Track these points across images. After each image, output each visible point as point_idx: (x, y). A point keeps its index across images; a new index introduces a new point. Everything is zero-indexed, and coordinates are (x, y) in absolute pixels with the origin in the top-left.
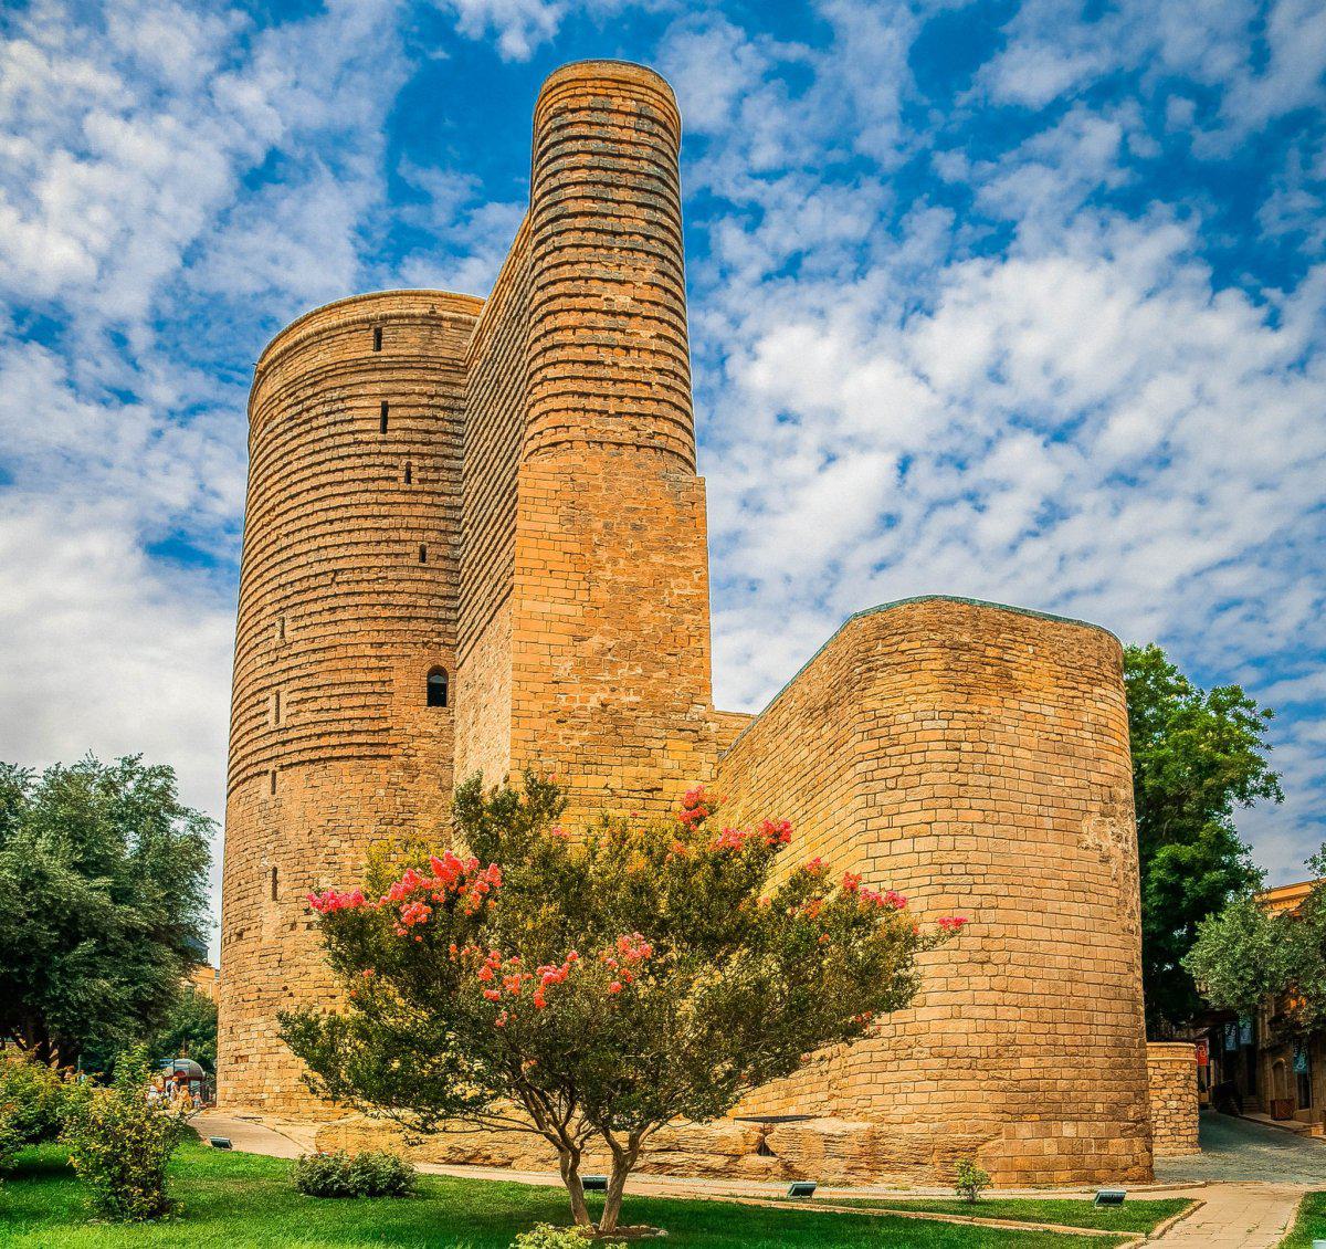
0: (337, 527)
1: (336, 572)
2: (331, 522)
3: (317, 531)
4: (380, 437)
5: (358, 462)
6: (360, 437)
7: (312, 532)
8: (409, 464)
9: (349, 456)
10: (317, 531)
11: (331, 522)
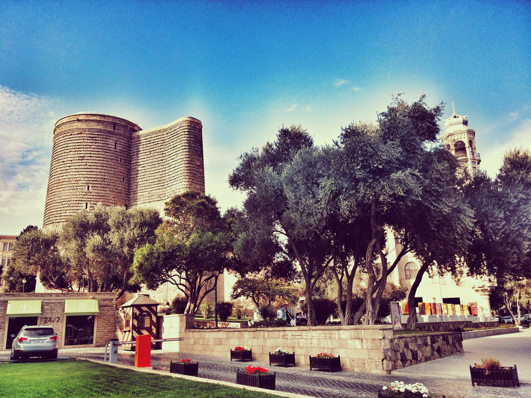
0: (104, 168)
1: (104, 179)
2: (103, 167)
3: (100, 168)
4: (115, 150)
5: (110, 154)
6: (111, 149)
7: (98, 167)
8: (121, 158)
9: (108, 152)
10: (100, 168)
11: (103, 167)
